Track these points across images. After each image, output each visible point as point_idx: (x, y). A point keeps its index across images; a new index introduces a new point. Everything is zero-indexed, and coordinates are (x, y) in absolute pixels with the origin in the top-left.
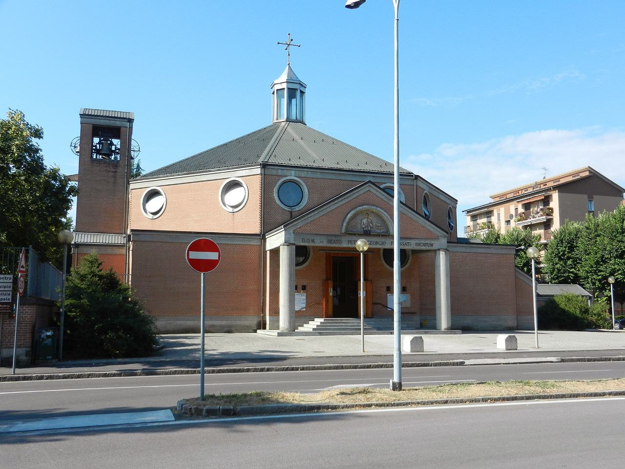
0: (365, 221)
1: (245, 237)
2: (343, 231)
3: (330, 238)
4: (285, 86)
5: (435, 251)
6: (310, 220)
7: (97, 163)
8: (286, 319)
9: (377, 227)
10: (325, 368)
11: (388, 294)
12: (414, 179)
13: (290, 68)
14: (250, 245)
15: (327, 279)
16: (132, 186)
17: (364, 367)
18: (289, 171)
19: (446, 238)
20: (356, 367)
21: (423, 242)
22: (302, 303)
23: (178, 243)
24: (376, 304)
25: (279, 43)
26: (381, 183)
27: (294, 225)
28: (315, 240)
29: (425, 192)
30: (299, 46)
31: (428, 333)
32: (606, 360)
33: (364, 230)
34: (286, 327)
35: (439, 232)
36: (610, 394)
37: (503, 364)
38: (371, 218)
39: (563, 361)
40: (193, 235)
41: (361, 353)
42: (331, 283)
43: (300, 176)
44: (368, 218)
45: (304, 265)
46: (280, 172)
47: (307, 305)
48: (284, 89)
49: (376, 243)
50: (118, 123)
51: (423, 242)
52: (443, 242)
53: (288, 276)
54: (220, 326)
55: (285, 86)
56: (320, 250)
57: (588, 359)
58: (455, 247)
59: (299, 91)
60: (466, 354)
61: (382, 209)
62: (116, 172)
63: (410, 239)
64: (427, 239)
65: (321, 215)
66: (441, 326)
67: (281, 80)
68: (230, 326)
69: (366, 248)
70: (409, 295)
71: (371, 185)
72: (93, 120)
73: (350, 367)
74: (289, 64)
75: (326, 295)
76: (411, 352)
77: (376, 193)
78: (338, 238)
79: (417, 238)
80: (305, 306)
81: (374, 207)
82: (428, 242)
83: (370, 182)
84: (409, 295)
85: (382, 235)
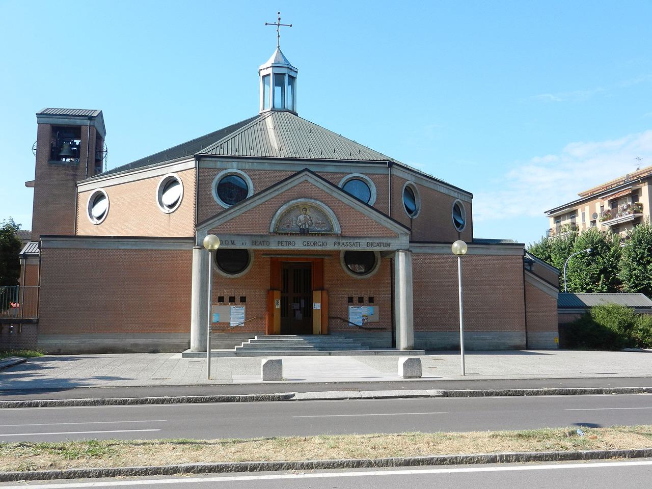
0: (302, 217)
1: (175, 241)
2: (272, 230)
3: (254, 239)
4: (270, 71)
5: (393, 252)
6: (229, 218)
7: (55, 166)
8: (196, 337)
9: (318, 225)
10: (78, 404)
11: (350, 307)
12: (389, 167)
13: (280, 52)
14: (181, 250)
15: (272, 289)
16: (80, 189)
17: (136, 402)
18: (230, 163)
19: (408, 236)
20: (124, 403)
21: (377, 241)
22: (240, 318)
23: (112, 250)
24: (334, 318)
25: (266, 24)
26: (345, 173)
27: (210, 224)
28: (235, 242)
29: (408, 182)
30: (291, 26)
31: (379, 354)
32: (516, 394)
33: (301, 229)
34: (196, 346)
35: (399, 229)
36: (189, 470)
37: (350, 399)
38: (309, 214)
39: (446, 395)
40: (113, 240)
41: (206, 381)
42: (277, 294)
43: (243, 168)
44: (305, 214)
45: (241, 273)
46: (219, 165)
47: (246, 319)
48: (269, 74)
49: (315, 244)
50: (78, 122)
51: (377, 241)
52: (405, 240)
53: (199, 286)
54: (144, 345)
55: (270, 71)
56: (263, 254)
57: (487, 392)
58: (443, 247)
59: (287, 77)
60: (335, 383)
61: (322, 202)
62: (76, 175)
63: (360, 237)
64: (383, 237)
65: (243, 211)
66: (400, 346)
67: (267, 66)
68: (156, 345)
69: (216, 247)
70: (377, 307)
71: (308, 173)
72: (51, 119)
73: (116, 403)
74: (279, 47)
75: (270, 309)
76: (264, 380)
77: (315, 183)
78: (265, 239)
79: (368, 237)
80: (243, 322)
81: (313, 200)
82: (384, 241)
83: (306, 170)
84: (377, 307)
85: (322, 234)
